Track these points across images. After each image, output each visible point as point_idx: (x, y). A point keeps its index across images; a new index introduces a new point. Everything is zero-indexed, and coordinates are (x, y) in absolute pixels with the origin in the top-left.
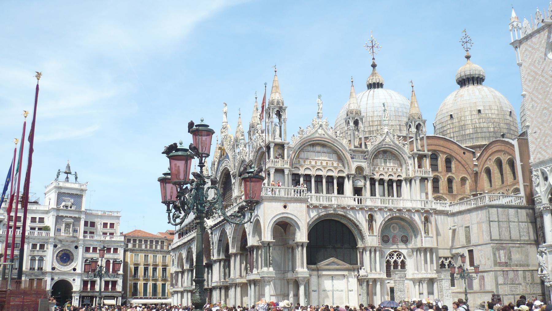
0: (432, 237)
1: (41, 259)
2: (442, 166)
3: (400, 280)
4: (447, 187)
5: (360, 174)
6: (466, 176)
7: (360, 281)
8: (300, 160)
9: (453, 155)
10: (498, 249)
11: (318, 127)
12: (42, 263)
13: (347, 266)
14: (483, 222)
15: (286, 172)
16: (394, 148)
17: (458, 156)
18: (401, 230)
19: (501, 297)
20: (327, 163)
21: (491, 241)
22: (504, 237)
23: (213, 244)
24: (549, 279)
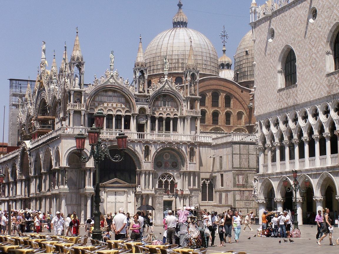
4: (224, 120)
5: (143, 113)
6: (242, 111)
8: (96, 103)
9: (231, 93)
10: (238, 175)
11: (110, 77)
13: (127, 184)
14: (229, 154)
15: (83, 114)
19: (237, 209)
20: (117, 105)
22: (243, 166)
23: (31, 163)
24: (258, 198)
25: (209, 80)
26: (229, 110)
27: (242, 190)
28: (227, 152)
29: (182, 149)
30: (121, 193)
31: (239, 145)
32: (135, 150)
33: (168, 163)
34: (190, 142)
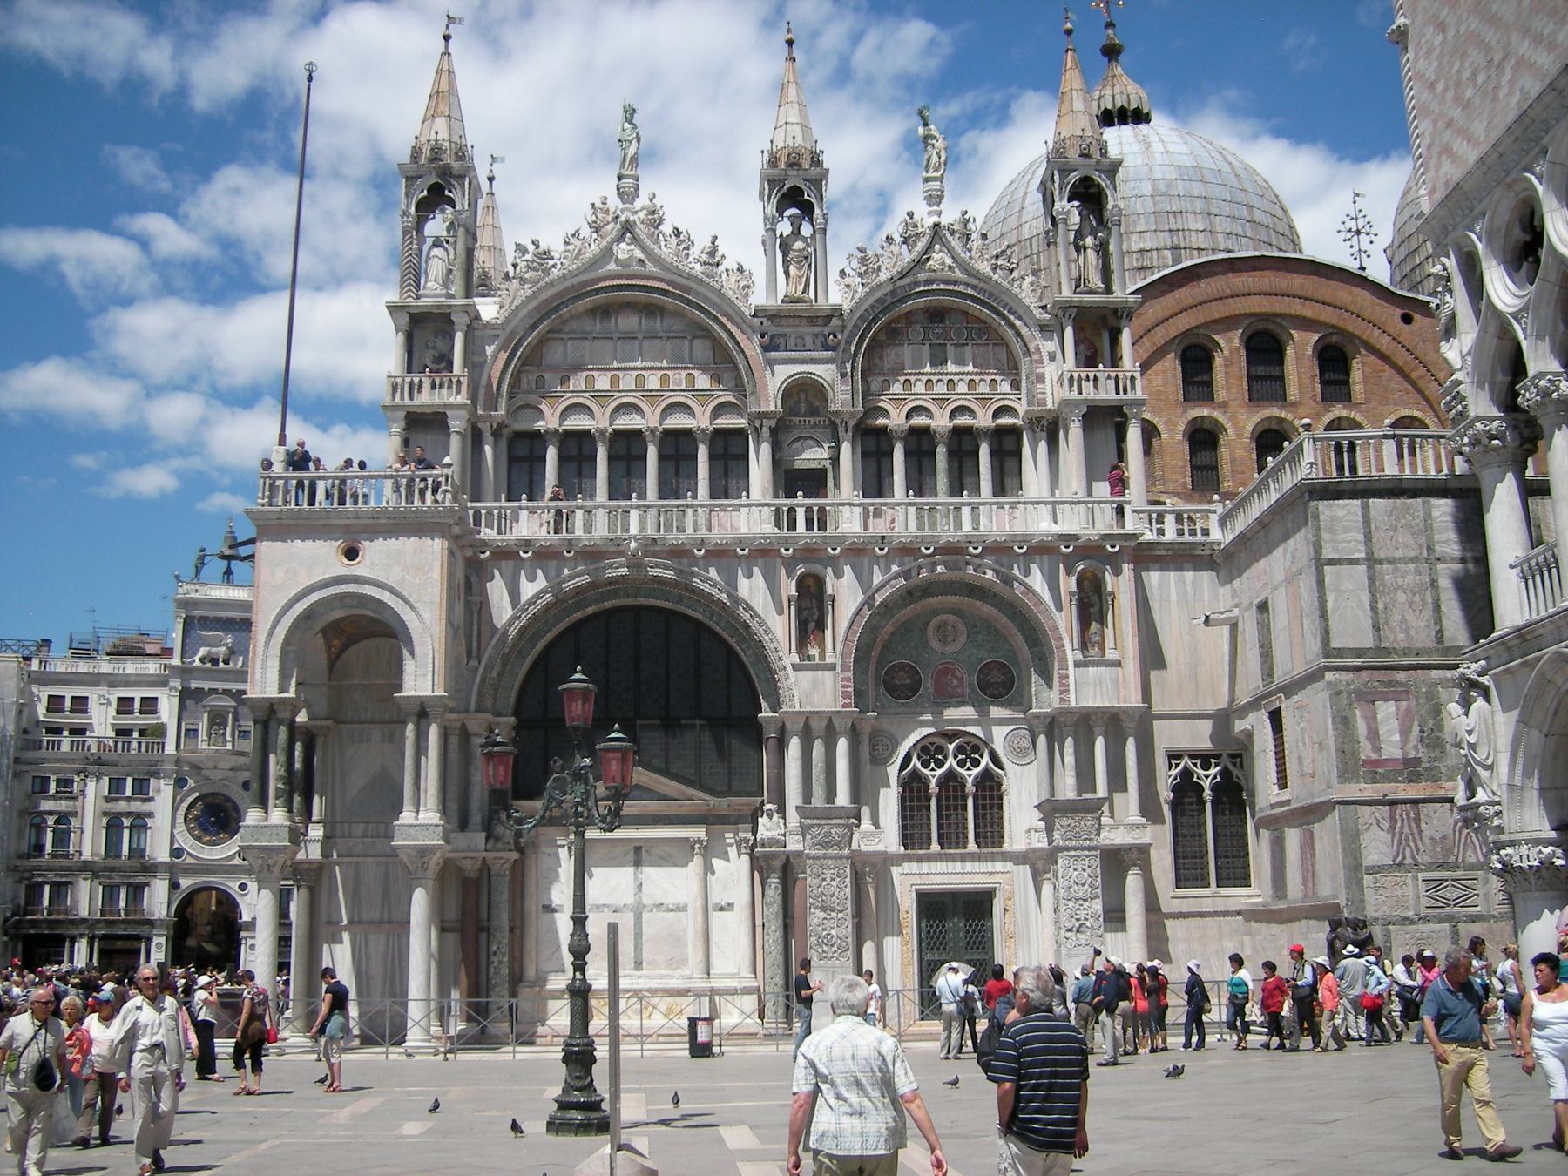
0: (1118, 664)
1: (140, 823)
2: (1300, 378)
3: (825, 857)
5: (813, 412)
6: (1416, 414)
7: (760, 864)
9: (1350, 328)
10: (1368, 698)
11: (614, 233)
12: (143, 836)
13: (699, 800)
15: (457, 424)
16: (969, 291)
17: (1377, 332)
18: (980, 638)
19: (1377, 931)
20: (664, 379)
21: (1327, 656)
22: (1401, 636)
24: (1500, 830)
25: (1224, 273)
26: (1344, 413)
27: (1402, 795)
28: (1288, 564)
29: (1027, 580)
30: (670, 856)
31: (1357, 502)
32: (736, 600)
33: (953, 672)
34: (1075, 537)
